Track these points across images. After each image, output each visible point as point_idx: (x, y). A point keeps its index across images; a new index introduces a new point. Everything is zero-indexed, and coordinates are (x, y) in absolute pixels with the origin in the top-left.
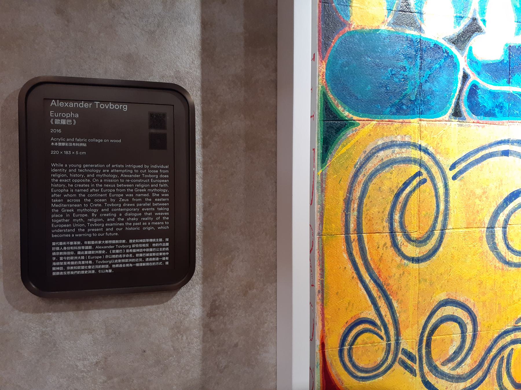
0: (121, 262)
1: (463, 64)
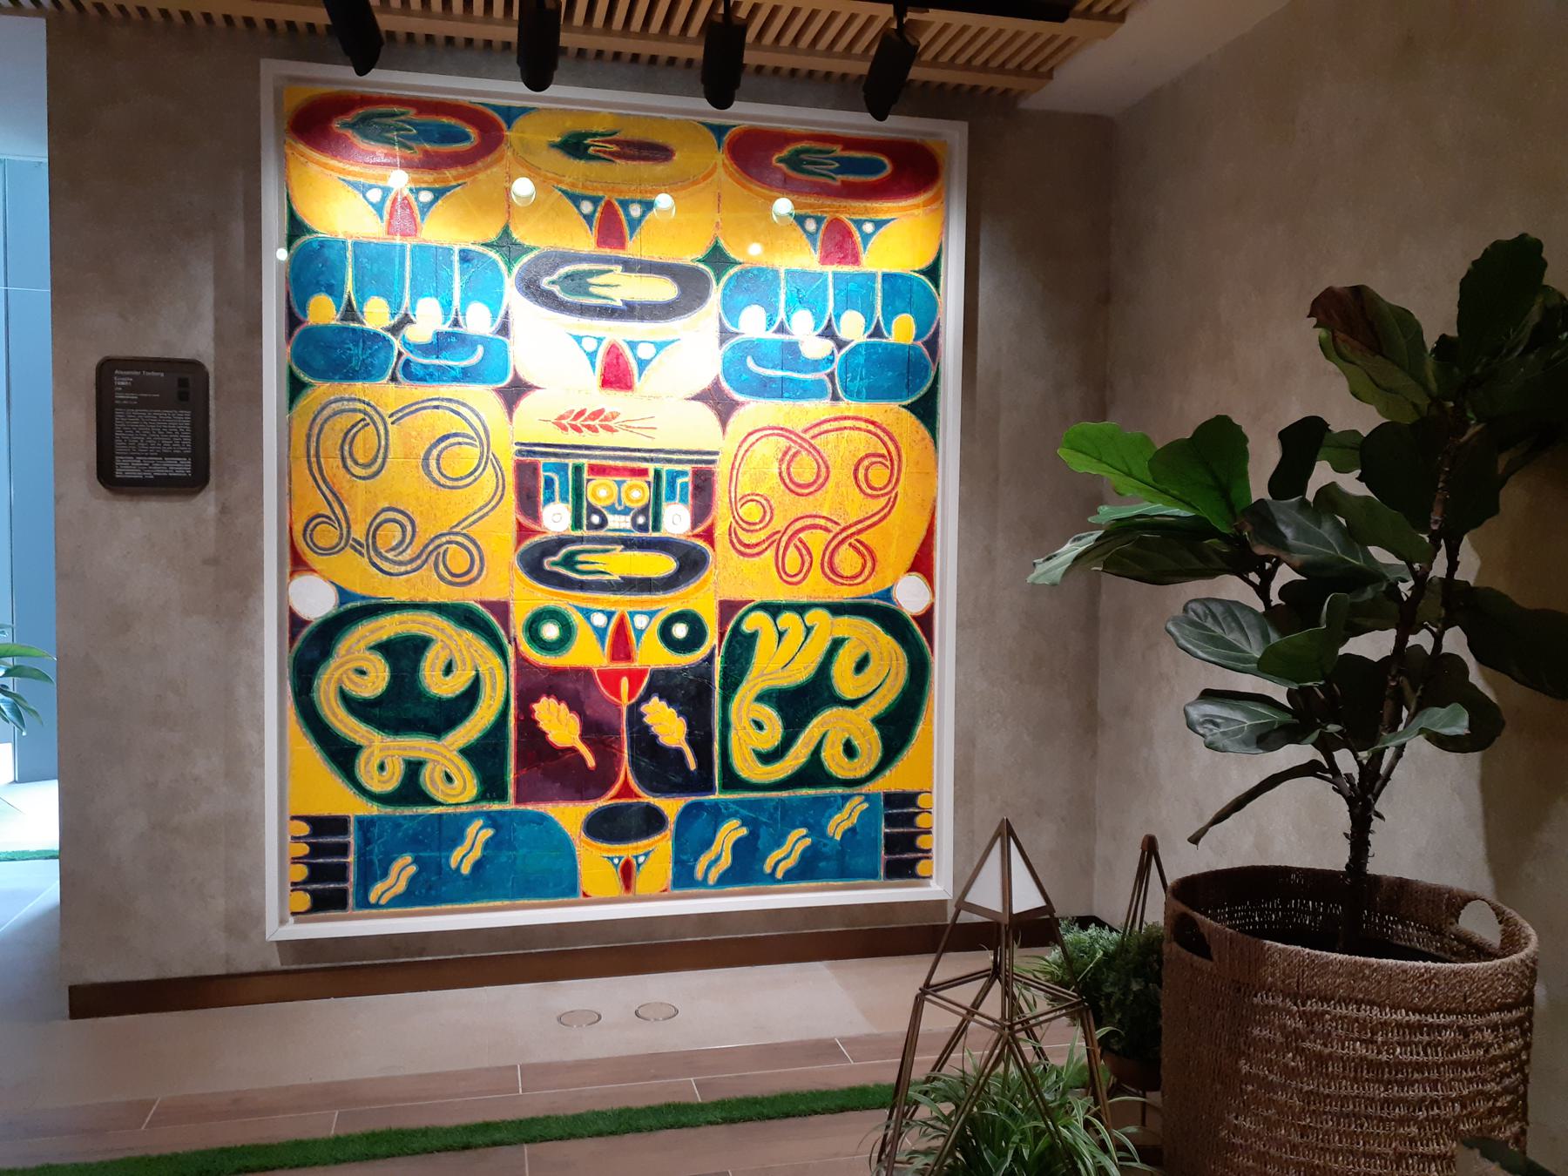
0: (159, 471)
1: (397, 344)
